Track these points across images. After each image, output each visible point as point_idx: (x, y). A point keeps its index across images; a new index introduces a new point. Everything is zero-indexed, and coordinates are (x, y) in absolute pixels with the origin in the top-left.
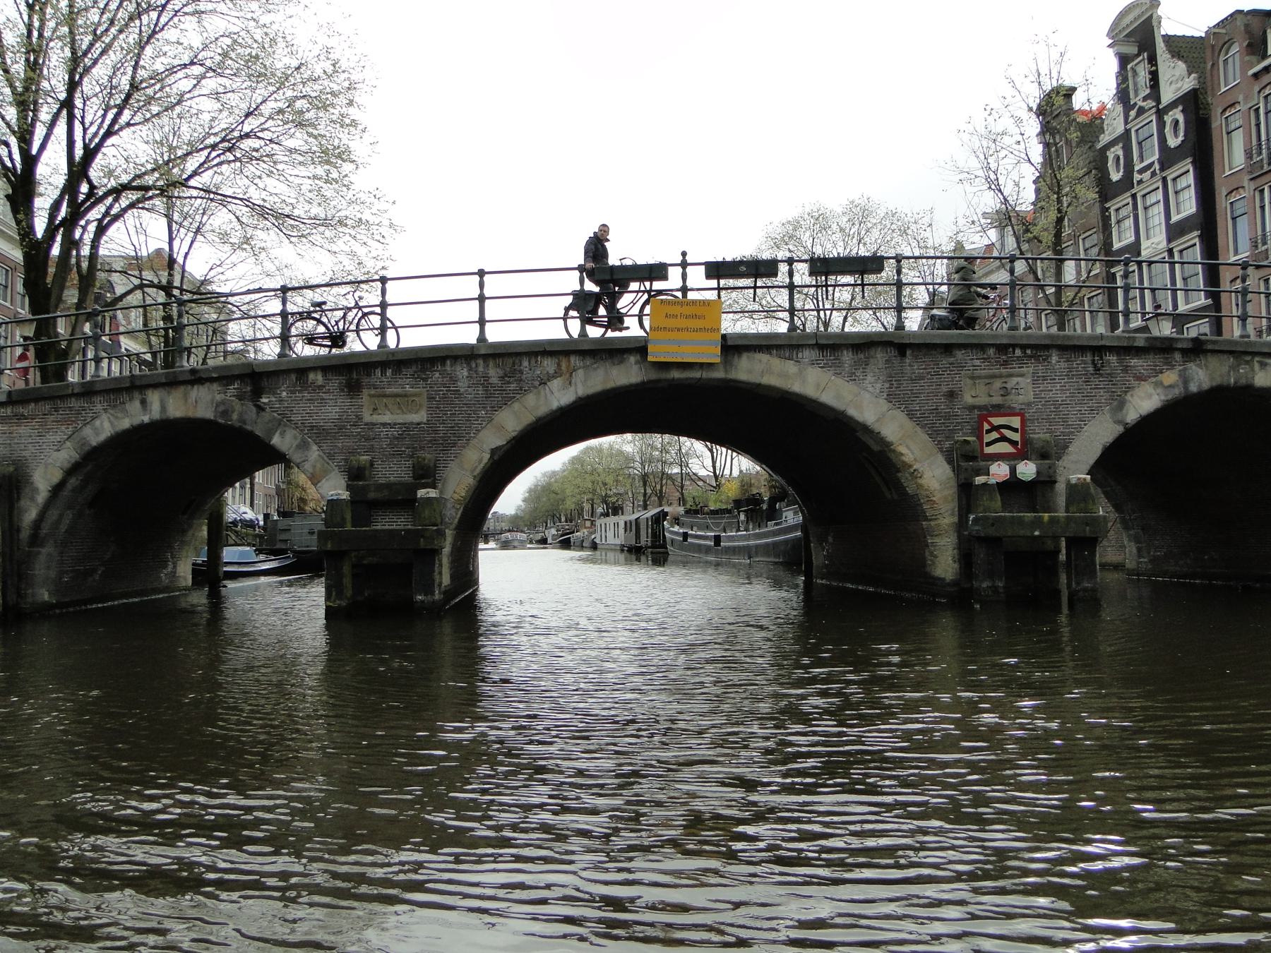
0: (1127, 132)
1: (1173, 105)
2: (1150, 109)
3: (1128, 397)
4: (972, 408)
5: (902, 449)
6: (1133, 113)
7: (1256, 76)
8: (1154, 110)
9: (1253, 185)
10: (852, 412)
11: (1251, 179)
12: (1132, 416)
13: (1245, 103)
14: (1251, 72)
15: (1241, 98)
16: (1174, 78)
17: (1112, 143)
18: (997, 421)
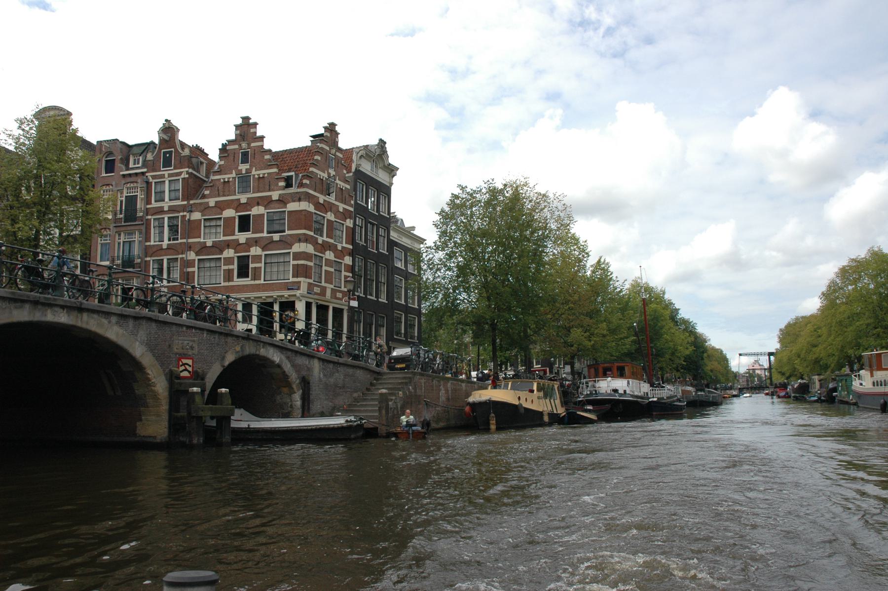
3: (226, 355)
4: (176, 354)
5: (149, 372)
7: (124, 176)
9: (115, 230)
10: (131, 351)
11: (115, 226)
12: (227, 363)
13: (116, 187)
14: (121, 173)
15: (114, 183)
18: (184, 361)
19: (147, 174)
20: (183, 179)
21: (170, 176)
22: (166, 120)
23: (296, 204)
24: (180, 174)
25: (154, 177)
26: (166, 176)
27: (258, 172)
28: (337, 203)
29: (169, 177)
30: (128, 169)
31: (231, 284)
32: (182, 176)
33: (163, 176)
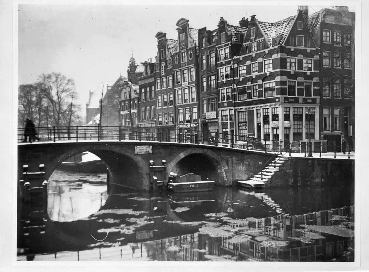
0: (180, 52)
1: (190, 49)
6: (181, 48)
13: (207, 54)
14: (208, 47)
19: (216, 47)
20: (230, 47)
21: (225, 46)
22: (221, 18)
23: (276, 54)
24: (228, 45)
25: (219, 48)
26: (223, 46)
27: (259, 39)
28: (305, 48)
29: (224, 47)
30: (210, 44)
31: (250, 100)
32: (229, 46)
33: (222, 47)
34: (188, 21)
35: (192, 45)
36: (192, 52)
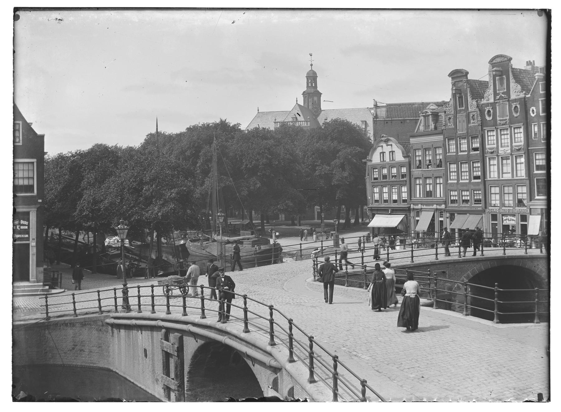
1: (515, 100)
2: (505, 98)
6: (498, 97)
8: (507, 99)
16: (517, 91)
17: (487, 105)
34: (511, 59)
35: (519, 95)
36: (518, 106)
